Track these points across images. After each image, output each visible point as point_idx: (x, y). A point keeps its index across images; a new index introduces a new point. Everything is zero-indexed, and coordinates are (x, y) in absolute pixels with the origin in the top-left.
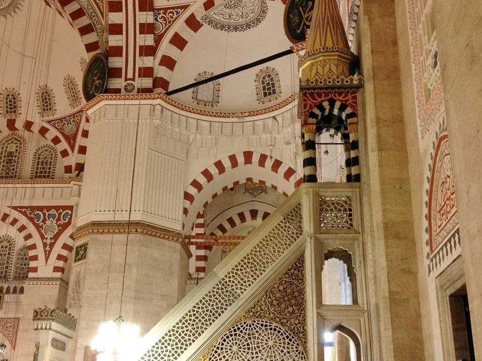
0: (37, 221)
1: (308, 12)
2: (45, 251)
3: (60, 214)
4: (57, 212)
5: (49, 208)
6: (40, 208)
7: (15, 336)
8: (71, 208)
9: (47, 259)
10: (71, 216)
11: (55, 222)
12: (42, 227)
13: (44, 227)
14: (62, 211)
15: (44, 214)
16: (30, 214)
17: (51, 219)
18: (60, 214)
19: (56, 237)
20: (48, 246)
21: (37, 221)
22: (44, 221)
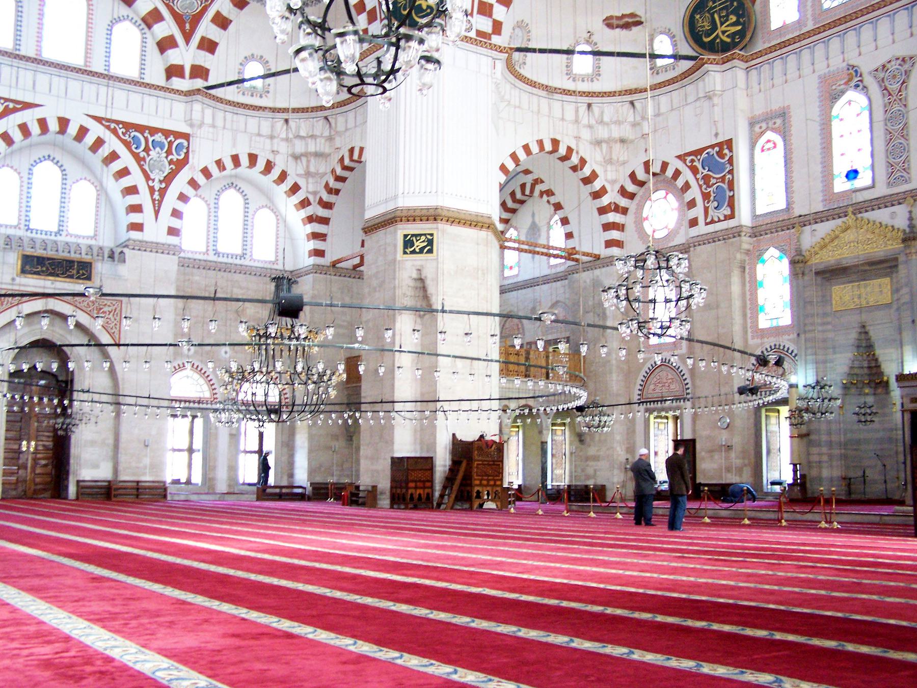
0: (136, 148)
1: (728, 26)
2: (154, 200)
3: (171, 143)
4: (166, 139)
5: (154, 131)
6: (141, 128)
7: (118, 327)
8: (186, 136)
9: (157, 213)
10: (188, 148)
11: (165, 155)
12: (144, 159)
13: (148, 160)
14: (173, 140)
15: (146, 139)
16: (124, 134)
17: (158, 149)
18: (171, 143)
19: (168, 180)
20: (157, 193)
21: (136, 148)
22: (147, 150)
